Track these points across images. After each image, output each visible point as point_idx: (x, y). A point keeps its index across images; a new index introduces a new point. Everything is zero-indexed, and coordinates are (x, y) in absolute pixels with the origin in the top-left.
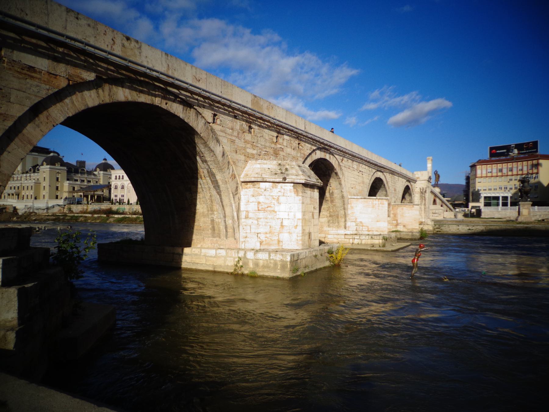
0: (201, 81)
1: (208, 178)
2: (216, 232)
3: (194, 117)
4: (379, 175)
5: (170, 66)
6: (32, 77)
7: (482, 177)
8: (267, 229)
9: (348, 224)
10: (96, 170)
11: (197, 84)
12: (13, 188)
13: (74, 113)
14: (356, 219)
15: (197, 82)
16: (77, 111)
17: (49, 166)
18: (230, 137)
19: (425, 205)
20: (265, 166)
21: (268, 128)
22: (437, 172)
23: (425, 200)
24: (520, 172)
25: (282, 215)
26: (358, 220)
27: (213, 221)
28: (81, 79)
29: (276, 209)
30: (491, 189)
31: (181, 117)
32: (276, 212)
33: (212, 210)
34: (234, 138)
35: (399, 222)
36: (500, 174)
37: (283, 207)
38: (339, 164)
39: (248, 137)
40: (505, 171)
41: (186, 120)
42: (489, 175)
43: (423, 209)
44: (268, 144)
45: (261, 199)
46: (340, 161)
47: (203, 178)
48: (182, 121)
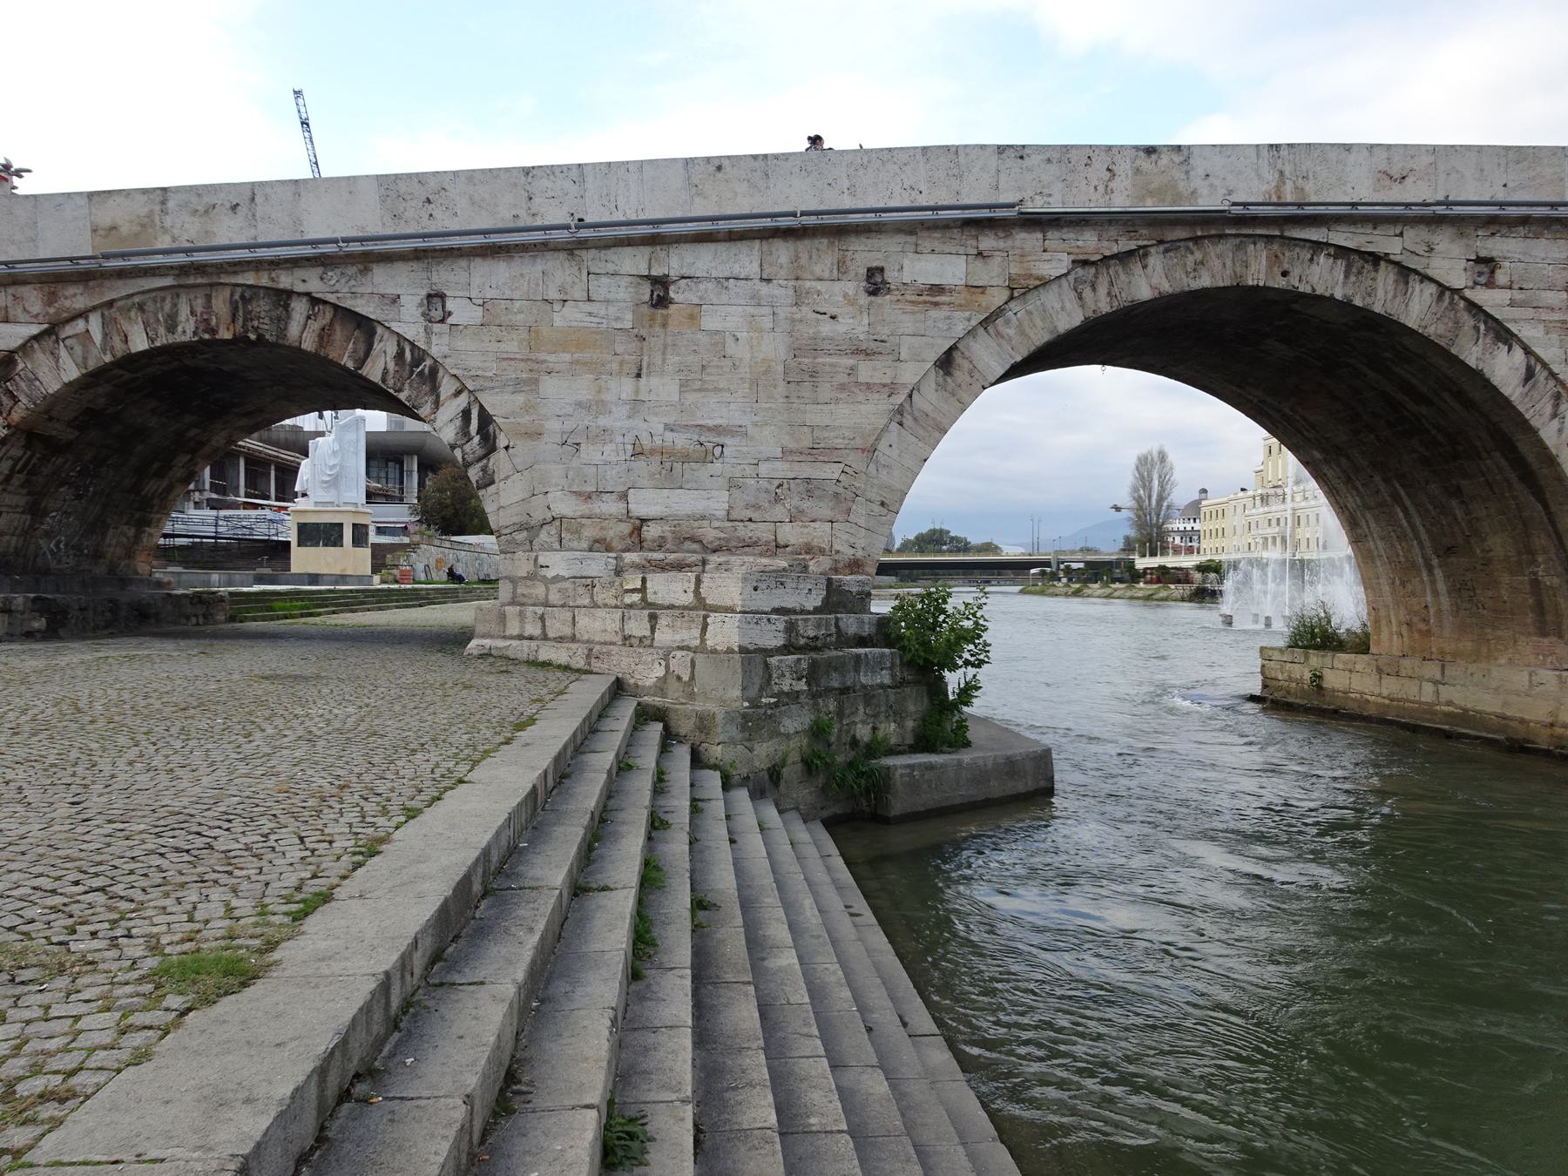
0: (1409, 181)
1: (1498, 454)
2: (1549, 617)
3: (1390, 288)
5: (1287, 173)
6: (936, 304)
11: (1397, 194)
12: (1274, 522)
13: (1026, 354)
15: (1396, 187)
16: (1033, 348)
18: (1556, 316)
27: (1536, 583)
28: (1038, 278)
31: (1338, 295)
33: (1531, 552)
41: (1358, 302)
47: (1484, 455)
48: (1346, 305)
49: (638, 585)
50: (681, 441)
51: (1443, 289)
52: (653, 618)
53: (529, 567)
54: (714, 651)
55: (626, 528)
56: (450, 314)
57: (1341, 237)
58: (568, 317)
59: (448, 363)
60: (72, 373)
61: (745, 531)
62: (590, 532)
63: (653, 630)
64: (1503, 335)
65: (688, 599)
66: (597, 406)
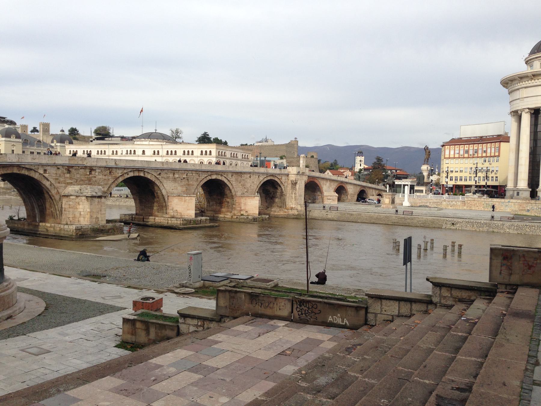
4: (214, 177)
7: (449, 158)
9: (168, 211)
10: (52, 142)
17: (4, 139)
24: (484, 155)
26: (175, 209)
30: (456, 172)
35: (242, 208)
36: (466, 155)
37: (81, 206)
39: (68, 175)
40: (471, 152)
42: (457, 156)
43: (294, 197)
45: (71, 203)
51: (40, 174)
57: (27, 166)
64: (48, 180)
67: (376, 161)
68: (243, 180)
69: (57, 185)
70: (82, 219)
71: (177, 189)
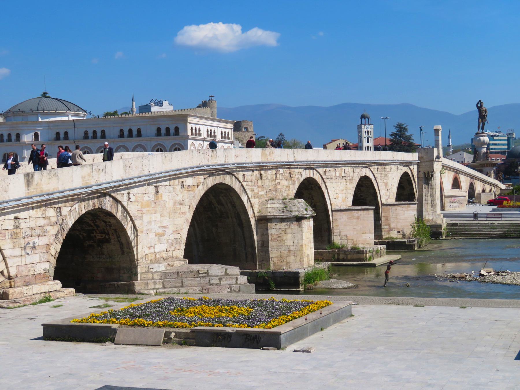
8: (278, 254)
14: (340, 232)
18: (250, 188)
19: (432, 195)
20: (274, 206)
21: (269, 169)
22: (481, 104)
23: (432, 189)
25: (290, 243)
26: (343, 234)
29: (284, 238)
32: (284, 241)
34: (252, 188)
35: (392, 226)
37: (289, 236)
38: (321, 176)
39: (260, 182)
43: (430, 201)
44: (270, 184)
46: (322, 174)
49: (206, 271)
50: (160, 231)
51: (240, 182)
52: (220, 279)
53: (147, 269)
54: (240, 284)
55: (154, 256)
56: (130, 198)
58: (146, 198)
59: (130, 212)
60: (73, 222)
61: (170, 254)
62: (150, 258)
63: (220, 282)
65: (223, 273)
66: (150, 222)
67: (395, 130)
68: (386, 175)
69: (253, 201)
70: (292, 258)
71: (338, 198)
